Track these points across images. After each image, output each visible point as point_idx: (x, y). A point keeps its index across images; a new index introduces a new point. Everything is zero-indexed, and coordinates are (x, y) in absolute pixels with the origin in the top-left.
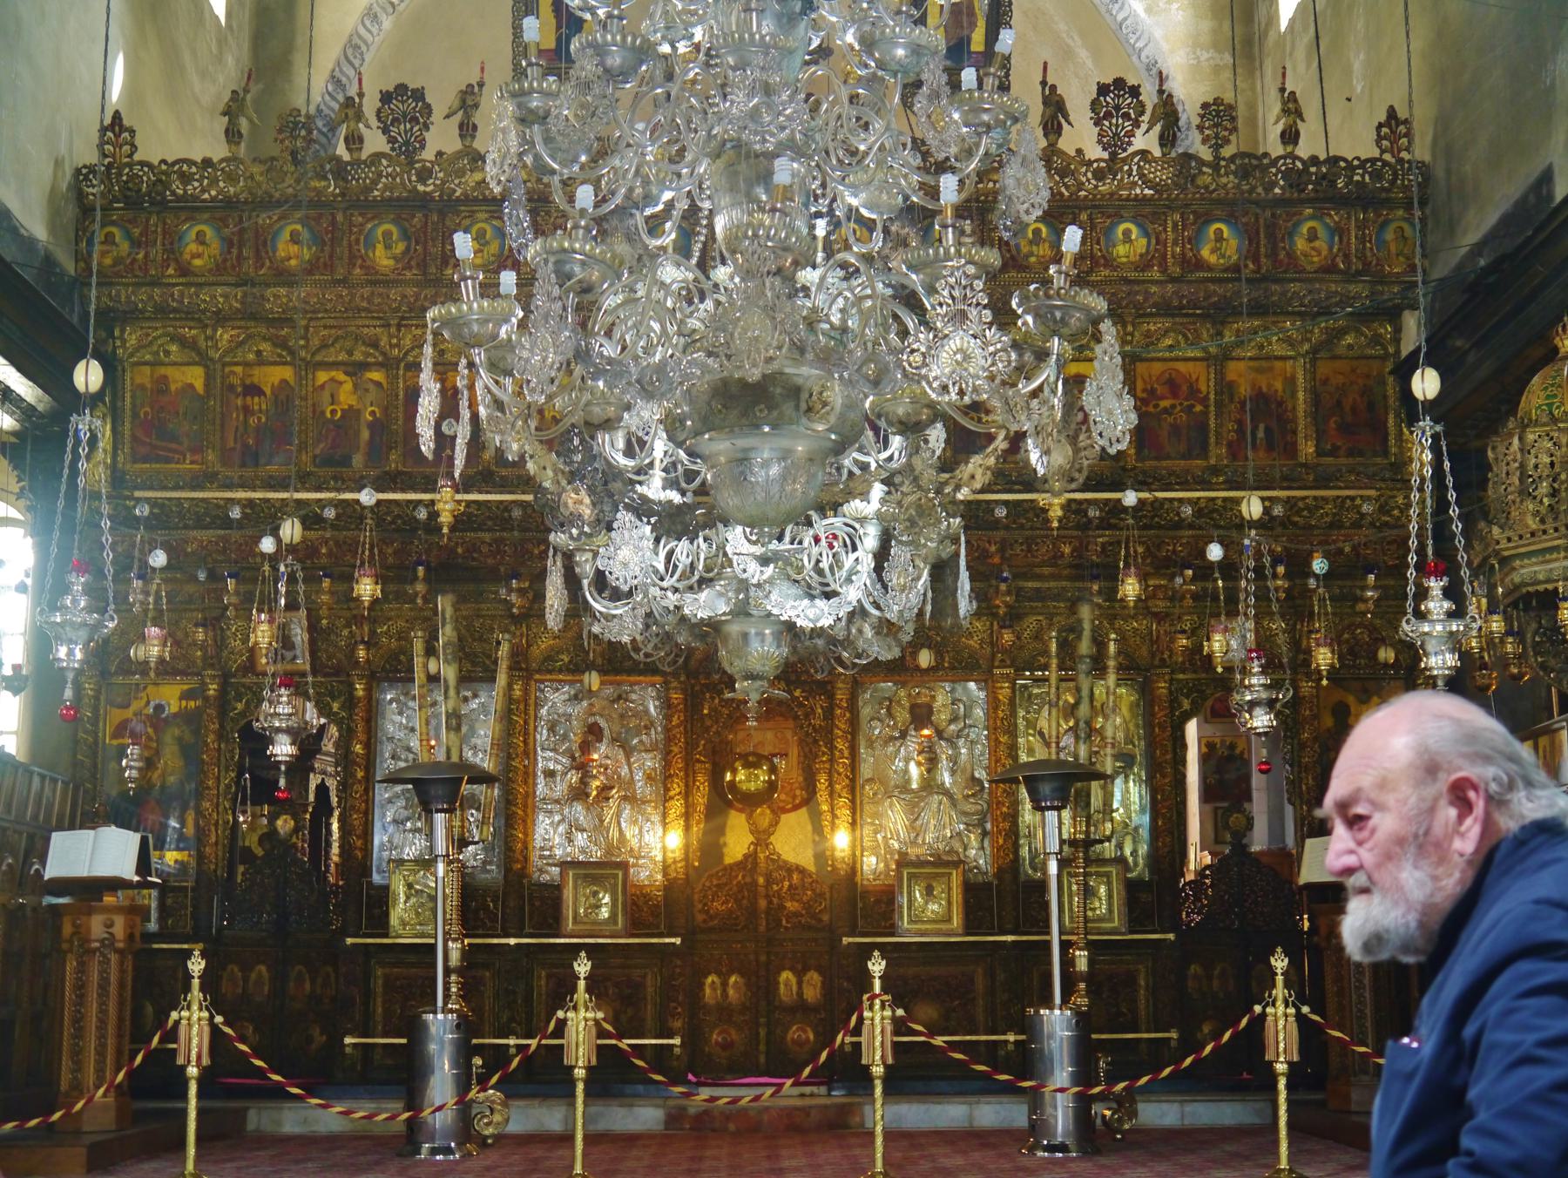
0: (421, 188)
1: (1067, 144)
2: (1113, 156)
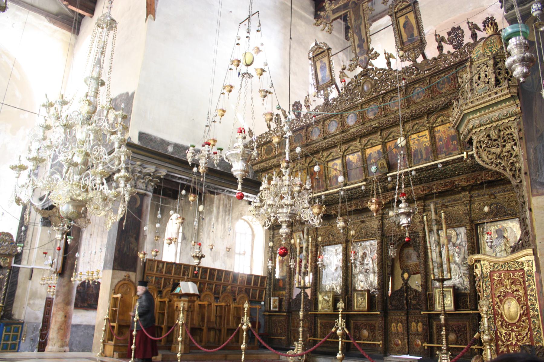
1: (445, 51)
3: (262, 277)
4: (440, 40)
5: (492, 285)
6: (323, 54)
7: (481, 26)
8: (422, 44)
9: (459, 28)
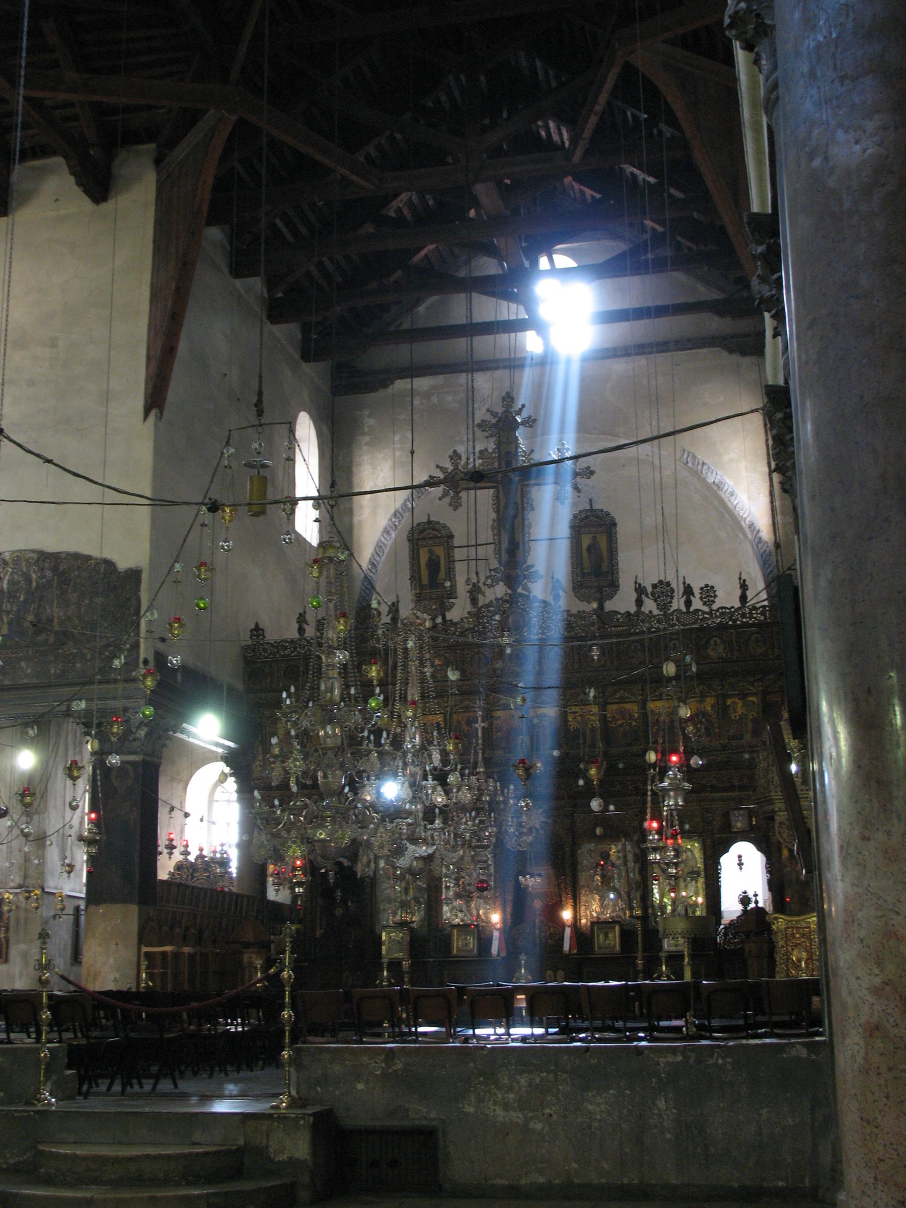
0: (377, 646)
2: (665, 615)
3: (249, 897)
4: (640, 590)
5: (786, 937)
6: (437, 541)
7: (696, 591)
8: (614, 586)
9: (668, 584)
